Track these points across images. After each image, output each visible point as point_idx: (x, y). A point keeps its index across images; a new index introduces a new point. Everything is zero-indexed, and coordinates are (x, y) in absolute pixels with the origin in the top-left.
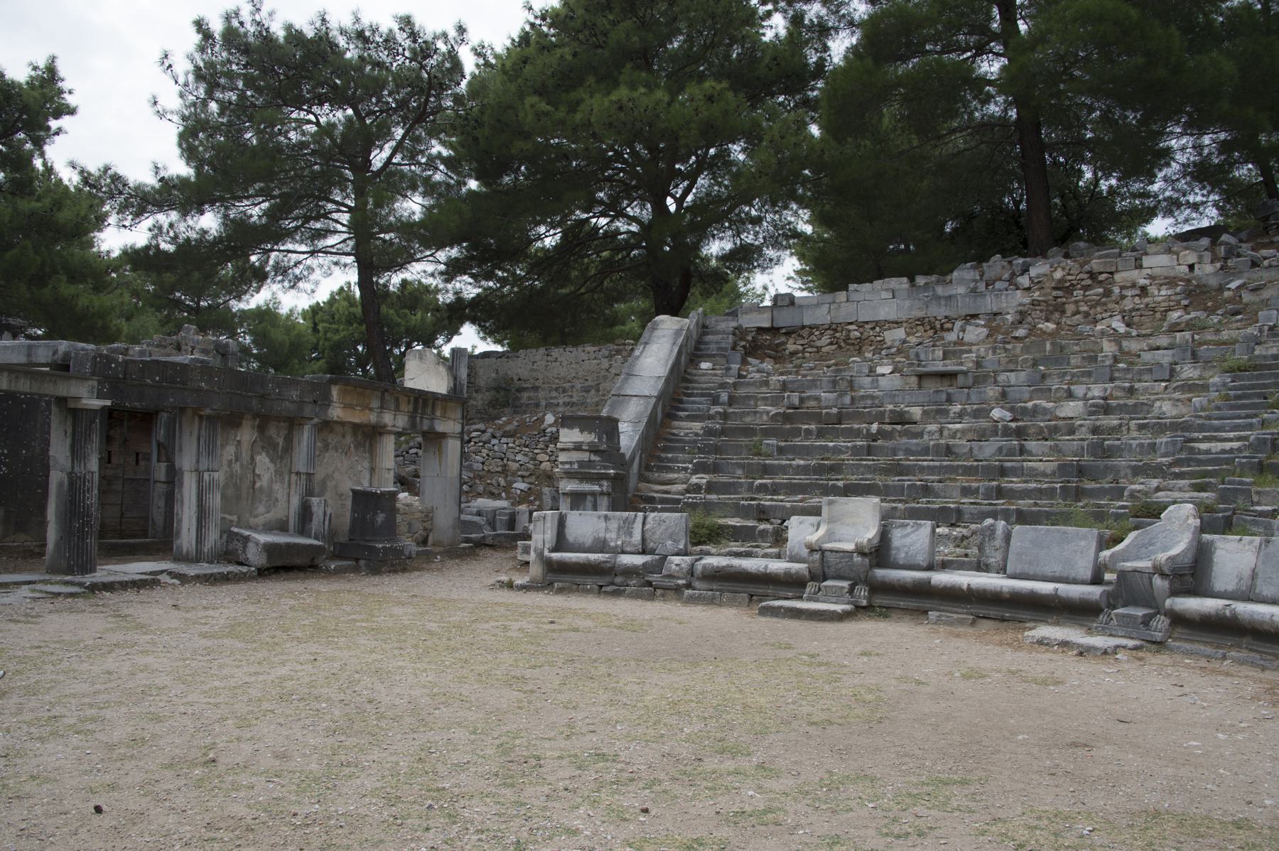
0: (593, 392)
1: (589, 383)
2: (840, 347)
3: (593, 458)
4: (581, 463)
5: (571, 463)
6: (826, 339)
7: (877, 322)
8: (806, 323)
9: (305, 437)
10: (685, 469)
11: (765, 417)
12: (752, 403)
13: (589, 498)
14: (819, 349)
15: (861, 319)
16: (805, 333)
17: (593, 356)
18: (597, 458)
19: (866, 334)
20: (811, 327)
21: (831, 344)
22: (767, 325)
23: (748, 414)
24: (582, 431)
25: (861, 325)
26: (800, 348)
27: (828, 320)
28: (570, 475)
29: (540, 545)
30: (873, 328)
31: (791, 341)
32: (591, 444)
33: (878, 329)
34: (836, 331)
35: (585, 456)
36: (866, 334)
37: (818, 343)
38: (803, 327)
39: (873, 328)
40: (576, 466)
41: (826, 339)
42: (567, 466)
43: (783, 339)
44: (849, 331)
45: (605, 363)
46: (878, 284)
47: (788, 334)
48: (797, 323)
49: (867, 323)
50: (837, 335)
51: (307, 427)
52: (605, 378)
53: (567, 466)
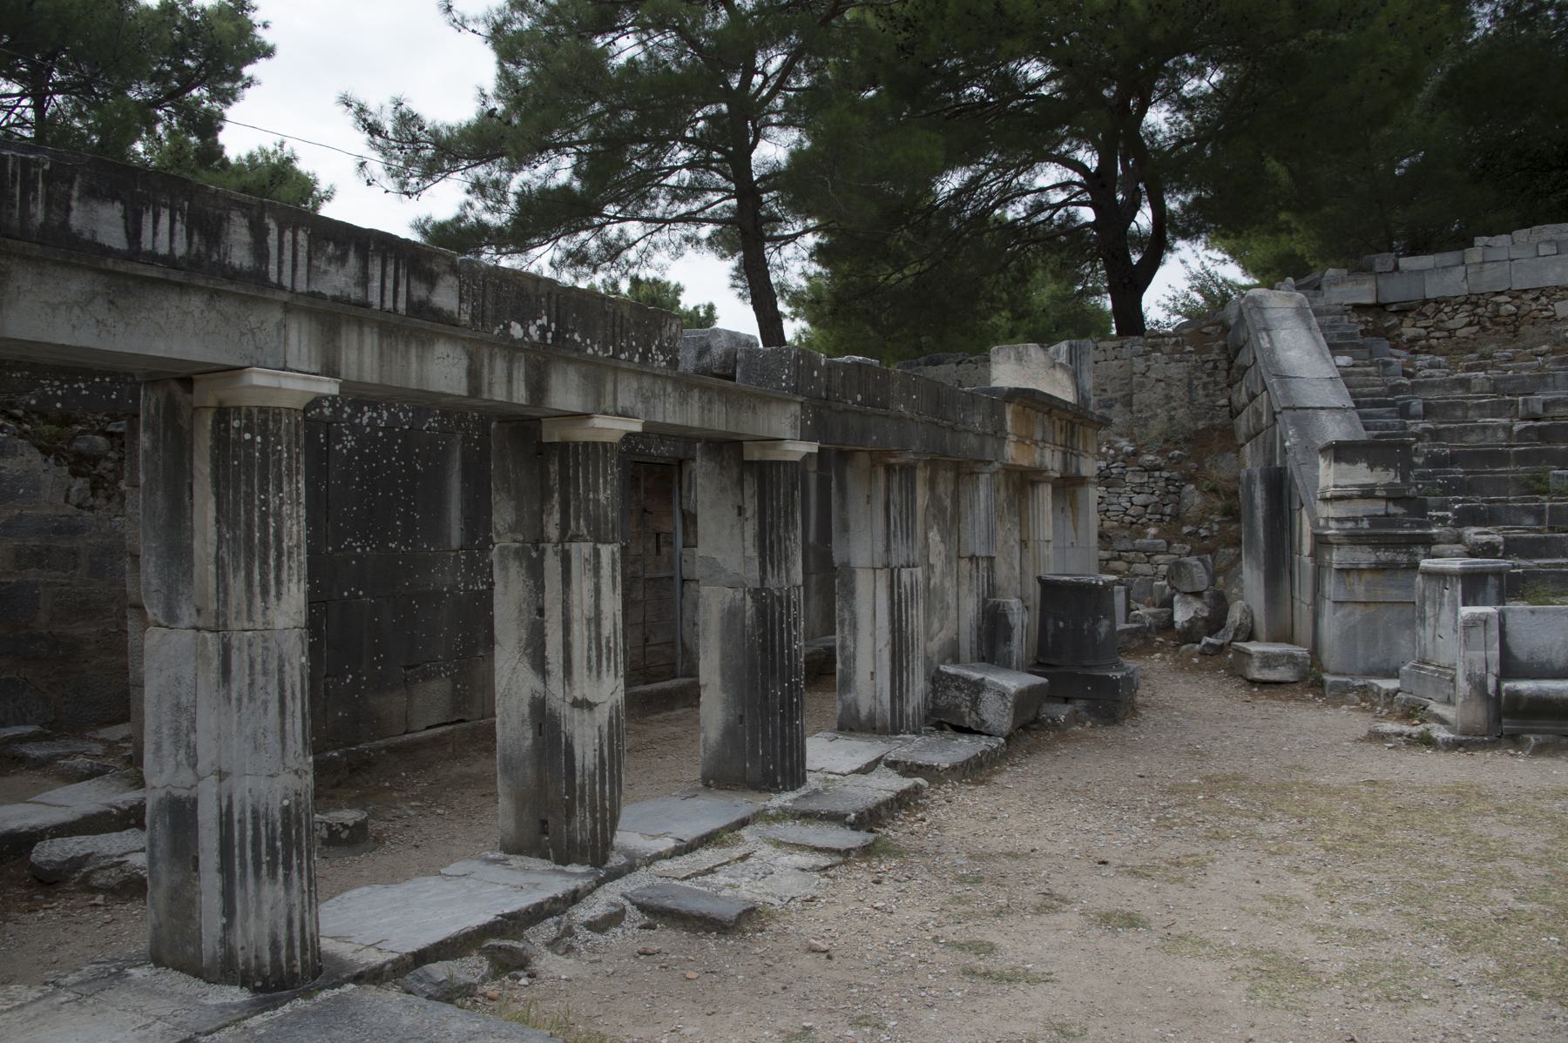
0: (1118, 407)
1: (1109, 394)
2: (1484, 329)
3: (1393, 509)
4: (1374, 519)
5: (1355, 519)
6: (1461, 318)
7: (1542, 291)
8: (1430, 294)
9: (983, 496)
10: (1443, 520)
11: (1501, 435)
12: (1459, 413)
13: (1492, 580)
14: (1451, 333)
15: (1517, 286)
16: (1429, 309)
17: (1111, 354)
18: (1400, 510)
19: (1525, 308)
20: (1436, 301)
21: (1470, 324)
22: (1369, 300)
23: (1472, 430)
24: (1372, 467)
25: (1515, 295)
26: (1423, 332)
27: (1464, 289)
28: (1355, 539)
29: (1479, 669)
30: (1537, 299)
31: (1408, 322)
32: (1389, 486)
33: (1544, 300)
34: (1476, 305)
35: (1378, 508)
36: (1525, 308)
37: (1451, 325)
38: (1426, 302)
39: (1537, 299)
40: (1365, 524)
41: (1461, 318)
42: (1349, 525)
43: (1395, 320)
44: (1498, 304)
45: (1140, 365)
46: (1521, 235)
47: (1403, 312)
48: (1415, 295)
49: (1525, 291)
50: (1479, 311)
51: (983, 478)
52: (1141, 385)
53: (1349, 525)
